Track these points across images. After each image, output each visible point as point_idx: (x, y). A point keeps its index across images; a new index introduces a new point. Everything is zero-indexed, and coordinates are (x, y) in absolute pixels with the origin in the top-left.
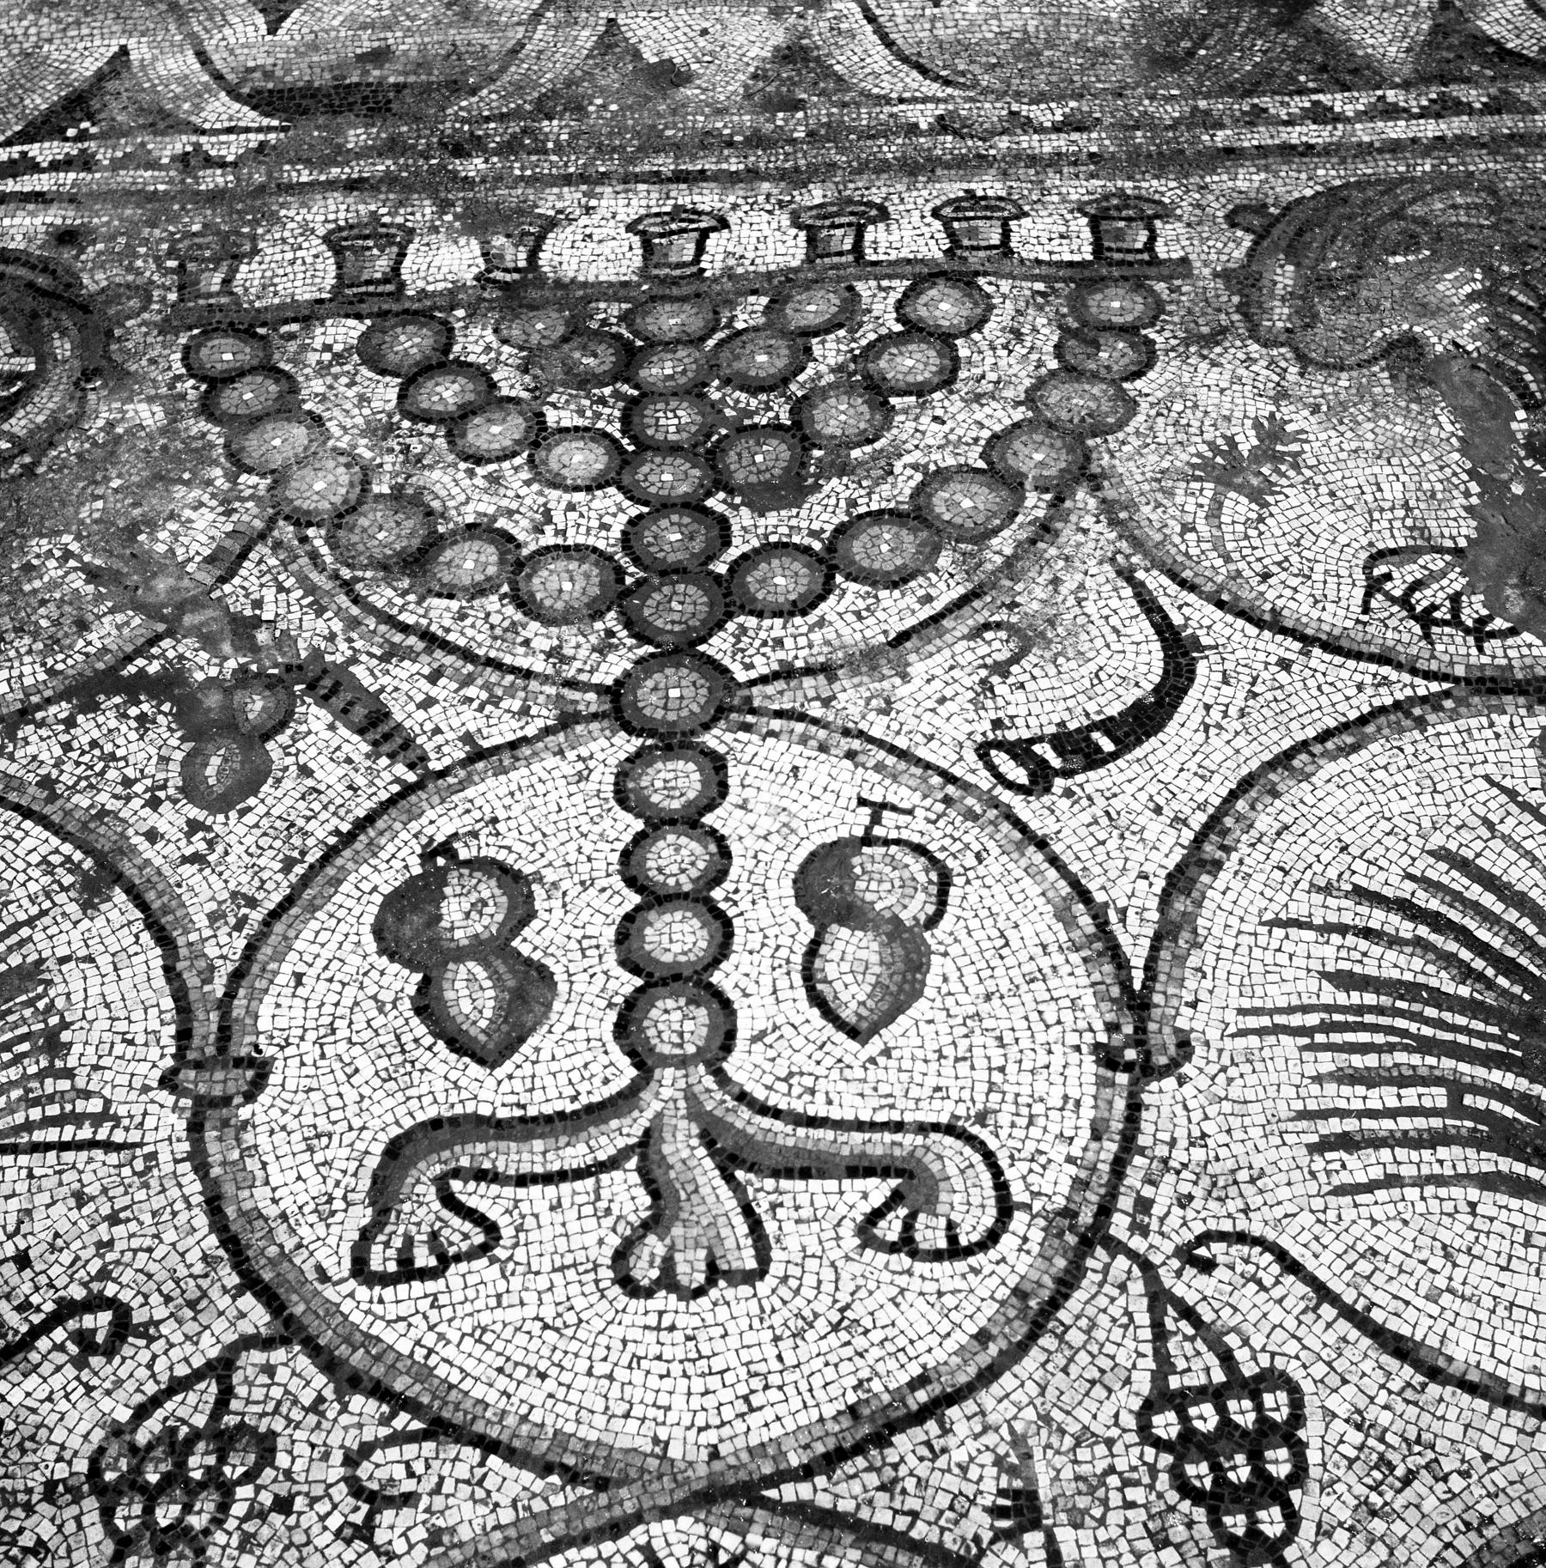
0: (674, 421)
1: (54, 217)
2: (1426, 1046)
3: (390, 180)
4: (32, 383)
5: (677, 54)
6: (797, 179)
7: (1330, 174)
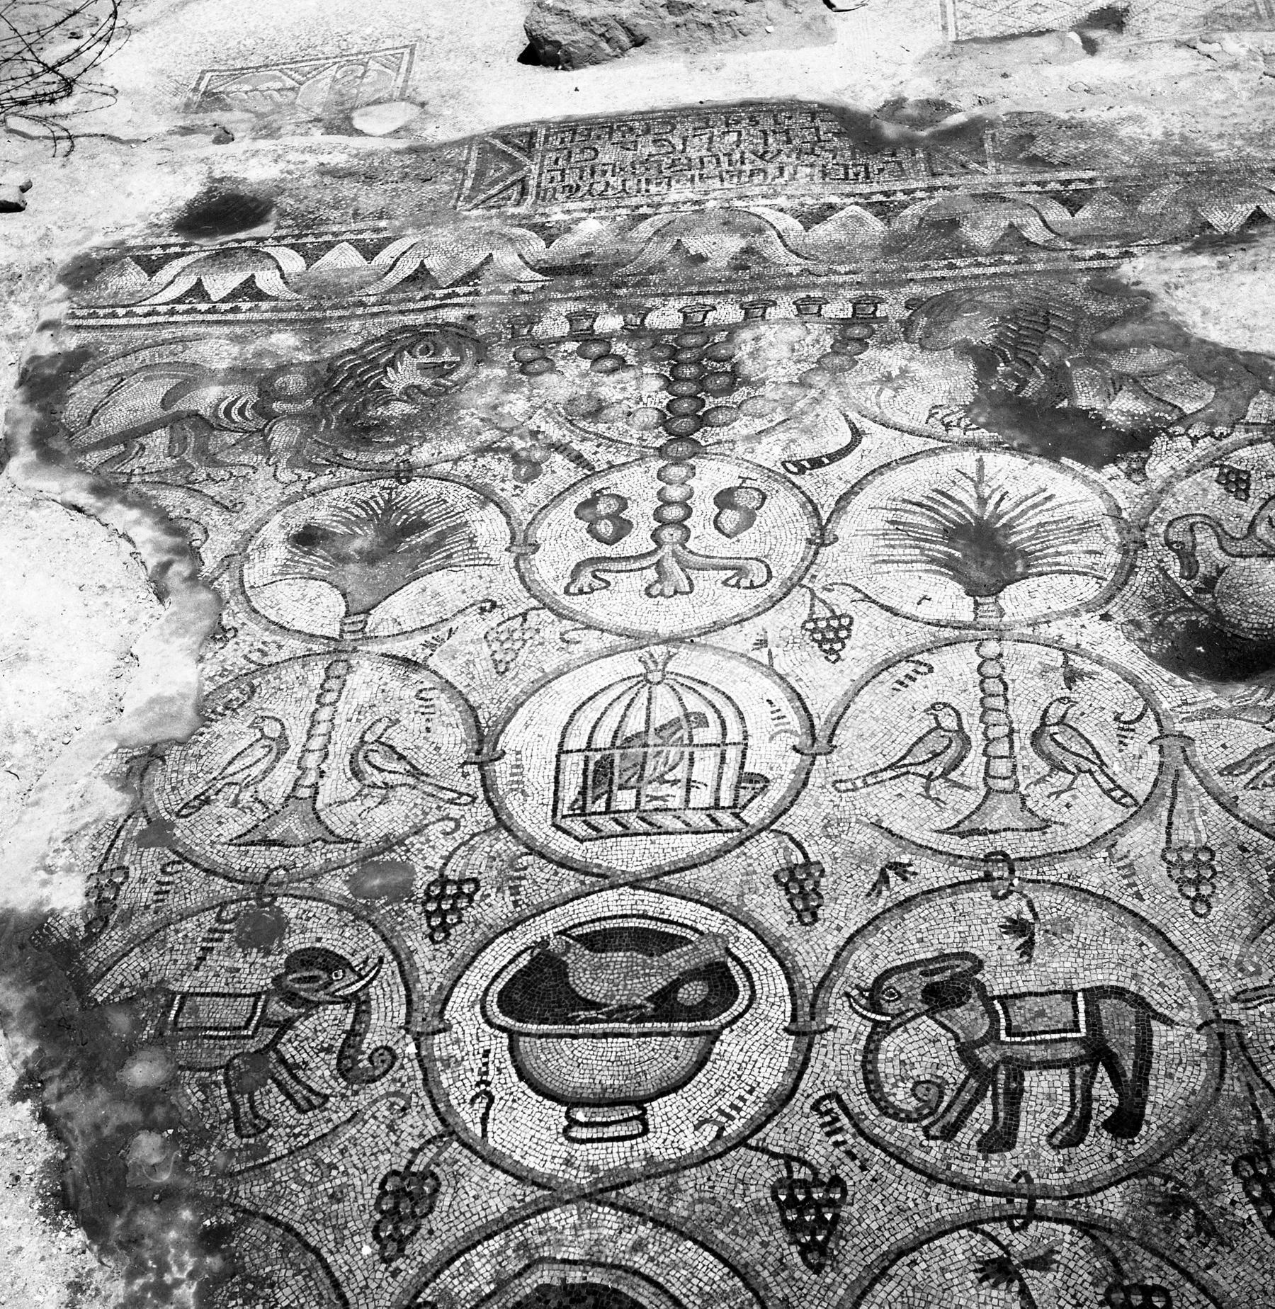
0: (689, 371)
1: (466, 311)
2: (916, 539)
3: (591, 297)
4: (458, 365)
5: (702, 251)
6: (743, 293)
7: (949, 286)
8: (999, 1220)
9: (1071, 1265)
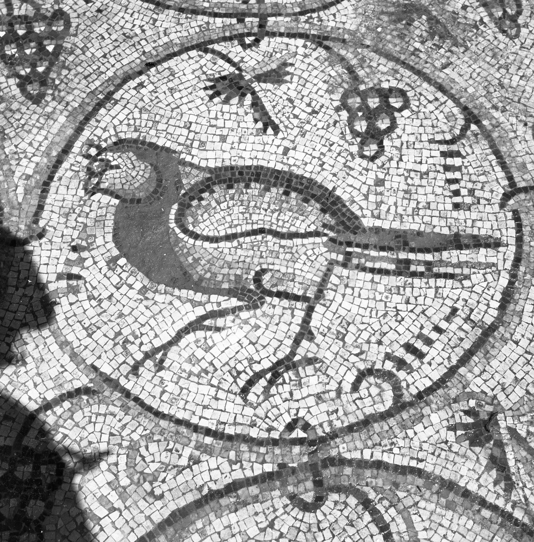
8: (231, 39)
9: (305, 75)
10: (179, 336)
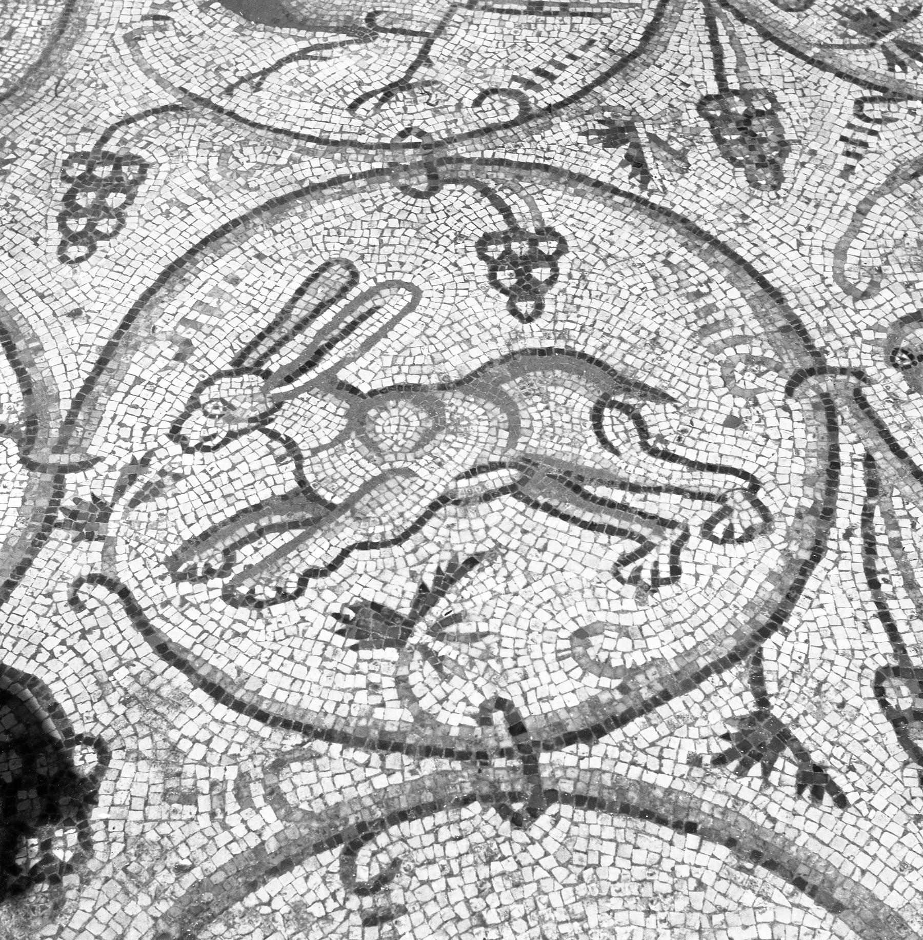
10: (280, 64)
